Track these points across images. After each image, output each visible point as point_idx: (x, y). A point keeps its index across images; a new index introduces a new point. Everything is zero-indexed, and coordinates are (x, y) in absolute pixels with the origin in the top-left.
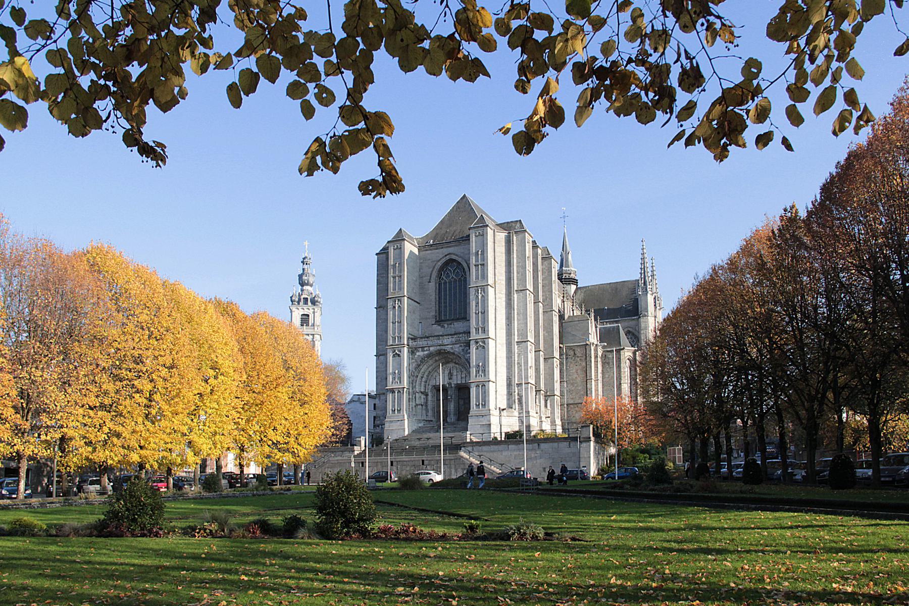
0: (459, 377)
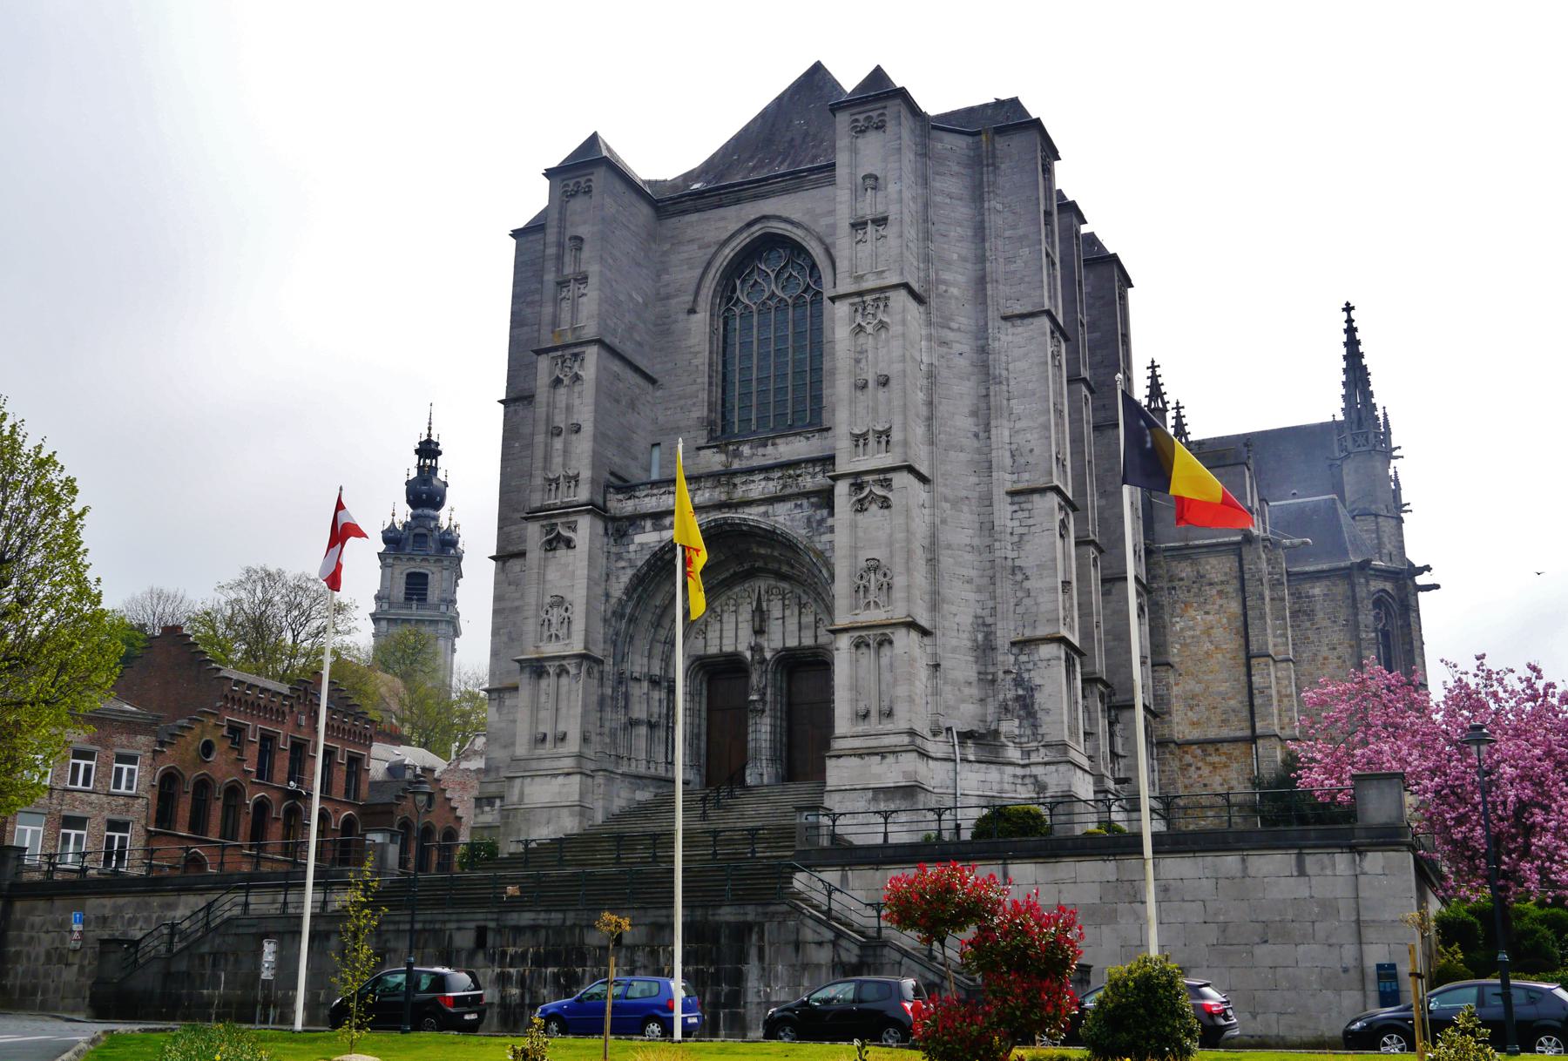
0: (792, 624)
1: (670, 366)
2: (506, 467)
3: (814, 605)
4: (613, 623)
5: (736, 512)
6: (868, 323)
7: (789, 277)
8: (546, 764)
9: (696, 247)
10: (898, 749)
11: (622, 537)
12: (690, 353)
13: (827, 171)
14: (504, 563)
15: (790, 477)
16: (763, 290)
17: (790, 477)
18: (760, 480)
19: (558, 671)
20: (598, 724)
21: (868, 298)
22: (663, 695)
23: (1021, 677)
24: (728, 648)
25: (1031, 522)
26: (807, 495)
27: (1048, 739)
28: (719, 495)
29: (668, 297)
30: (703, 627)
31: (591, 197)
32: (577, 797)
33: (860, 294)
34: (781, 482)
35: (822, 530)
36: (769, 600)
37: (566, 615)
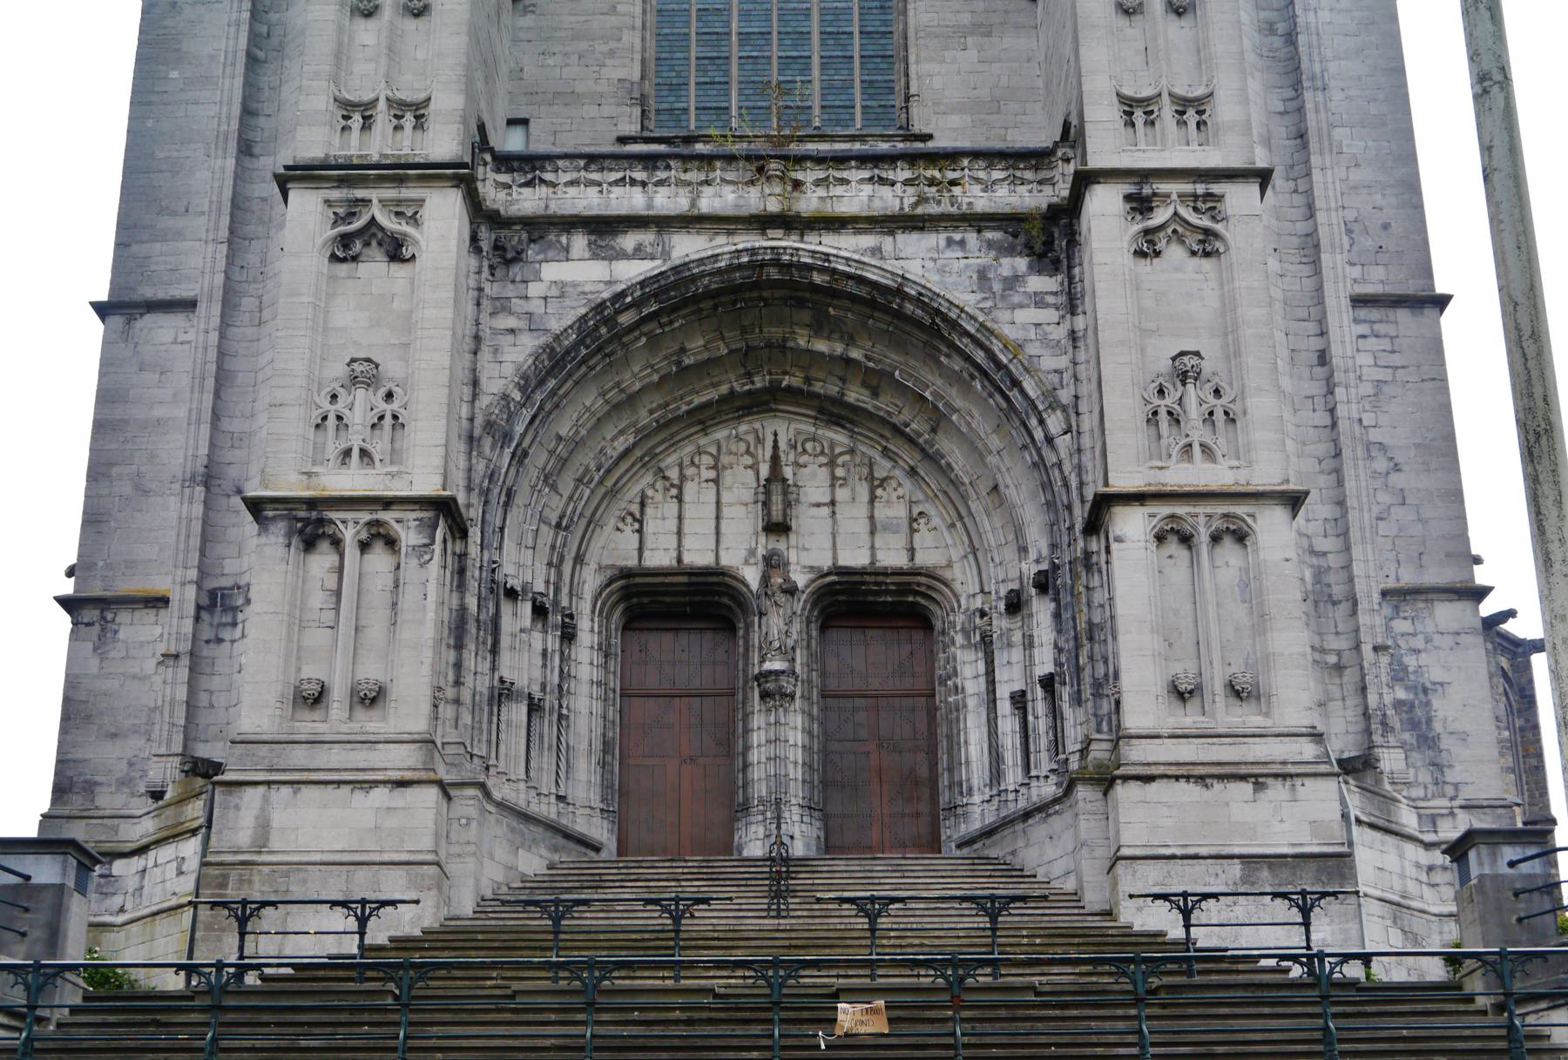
0: (854, 517)
3: (908, 484)
4: (487, 450)
5: (802, 241)
8: (335, 757)
10: (1292, 769)
11: (508, 263)
15: (932, 182)
17: (932, 182)
18: (862, 181)
19: (364, 536)
20: (451, 678)
22: (553, 642)
23: (1400, 663)
24: (698, 555)
27: (1467, 793)
30: (635, 508)
32: (427, 843)
34: (910, 190)
35: (1016, 299)
37: (388, 409)
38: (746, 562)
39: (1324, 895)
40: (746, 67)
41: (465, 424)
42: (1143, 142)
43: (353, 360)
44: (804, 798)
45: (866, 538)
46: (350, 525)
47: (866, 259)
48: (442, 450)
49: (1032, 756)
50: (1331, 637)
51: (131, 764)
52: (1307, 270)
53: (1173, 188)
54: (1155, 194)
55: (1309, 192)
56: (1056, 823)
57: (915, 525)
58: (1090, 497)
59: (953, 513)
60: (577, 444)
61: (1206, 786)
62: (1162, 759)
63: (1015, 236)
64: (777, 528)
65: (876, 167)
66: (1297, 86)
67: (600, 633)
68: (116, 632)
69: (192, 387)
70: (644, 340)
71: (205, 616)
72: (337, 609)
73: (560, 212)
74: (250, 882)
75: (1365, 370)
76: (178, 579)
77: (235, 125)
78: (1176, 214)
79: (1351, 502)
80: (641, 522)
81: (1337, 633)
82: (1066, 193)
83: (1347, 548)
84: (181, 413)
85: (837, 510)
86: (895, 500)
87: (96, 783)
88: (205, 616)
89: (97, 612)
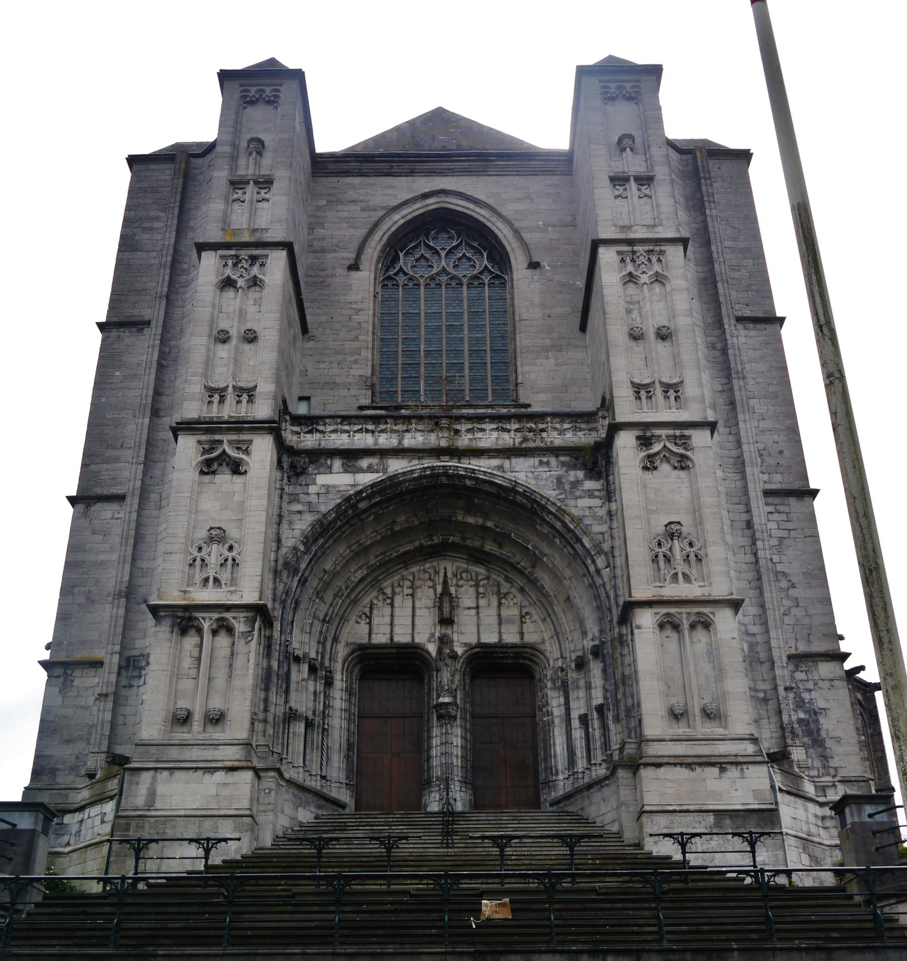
0: (489, 615)
1: (324, 318)
2: (101, 397)
3: (519, 598)
4: (285, 579)
5: (459, 462)
6: (644, 272)
7: (460, 259)
9: (358, 208)
10: (740, 759)
11: (298, 475)
12: (351, 308)
13: (518, 160)
14: (88, 506)
15: (531, 430)
16: (432, 267)
17: (531, 430)
18: (492, 430)
19: (215, 626)
20: (262, 707)
21: (639, 248)
22: (320, 687)
23: (801, 698)
25: (790, 525)
26: (556, 451)
27: (842, 773)
28: (434, 440)
29: (323, 251)
30: (367, 610)
31: (276, 108)
32: (246, 804)
33: (631, 242)
34: (519, 434)
35: (578, 493)
36: (457, 586)
37: (230, 555)
38: (429, 641)
39: (762, 834)
40: (429, 369)
41: (273, 563)
42: (646, 408)
43: (211, 528)
44: (462, 777)
45: (496, 626)
46: (207, 620)
47: (495, 472)
48: (259, 578)
49: (592, 752)
50: (760, 683)
51: (77, 758)
52: (738, 476)
53: (663, 432)
54: (653, 436)
55: (738, 434)
56: (607, 791)
57: (524, 620)
58: (621, 603)
59: (544, 612)
60: (334, 575)
61: (692, 769)
62: (667, 753)
63: (577, 459)
64: (446, 621)
65: (500, 422)
66: (729, 377)
67: (346, 681)
68: (73, 681)
69: (121, 543)
70: (372, 517)
71: (123, 672)
72: (198, 668)
73: (326, 447)
74: (143, 827)
75: (773, 531)
76: (109, 651)
77: (150, 400)
78: (665, 446)
79: (768, 605)
80: (370, 618)
81: (764, 680)
82: (604, 436)
83: (767, 631)
84: (114, 557)
85: (480, 611)
86: (512, 605)
87: (57, 769)
88: (123, 672)
89: (62, 670)
